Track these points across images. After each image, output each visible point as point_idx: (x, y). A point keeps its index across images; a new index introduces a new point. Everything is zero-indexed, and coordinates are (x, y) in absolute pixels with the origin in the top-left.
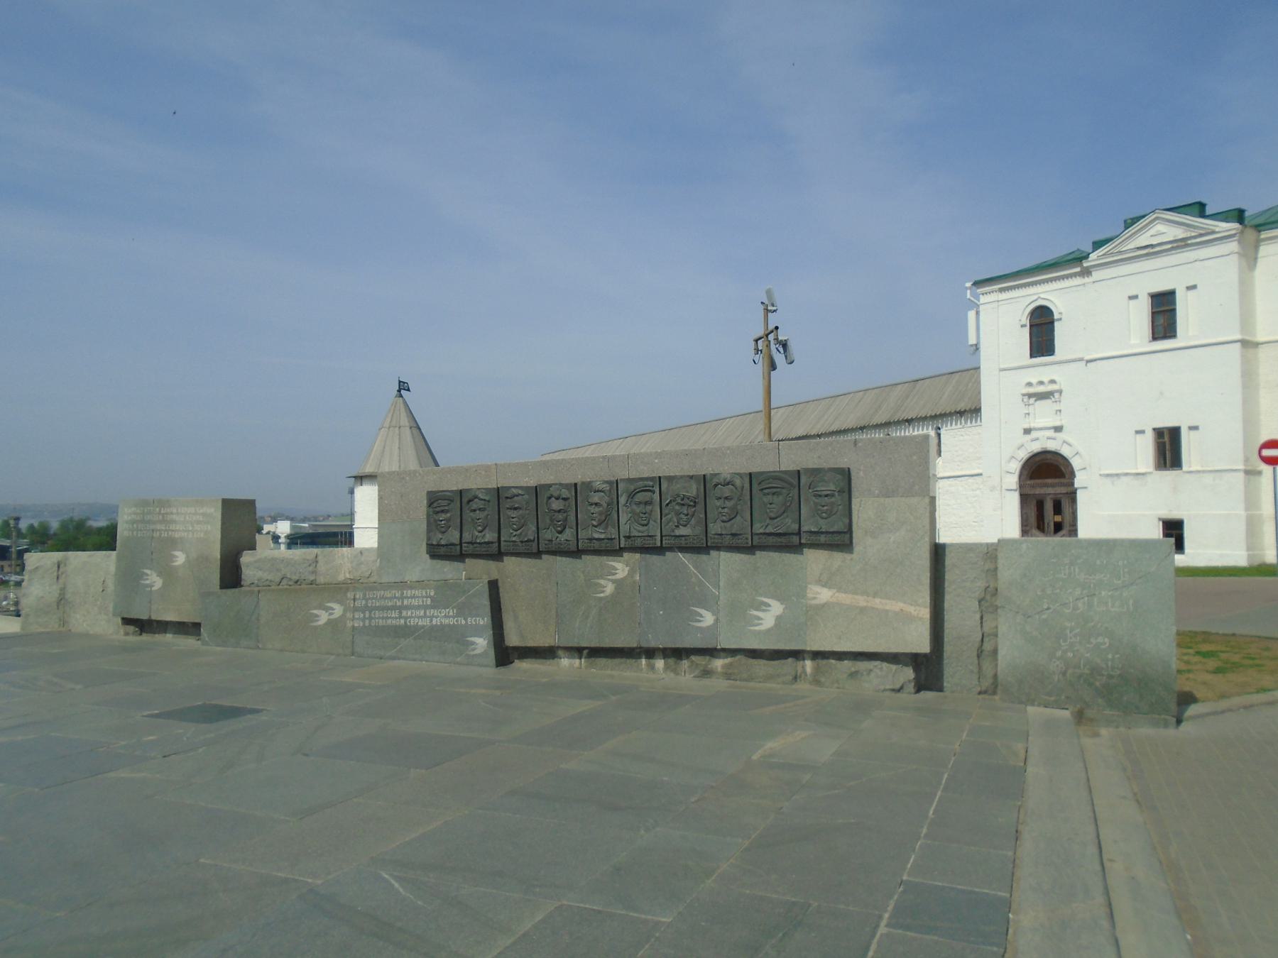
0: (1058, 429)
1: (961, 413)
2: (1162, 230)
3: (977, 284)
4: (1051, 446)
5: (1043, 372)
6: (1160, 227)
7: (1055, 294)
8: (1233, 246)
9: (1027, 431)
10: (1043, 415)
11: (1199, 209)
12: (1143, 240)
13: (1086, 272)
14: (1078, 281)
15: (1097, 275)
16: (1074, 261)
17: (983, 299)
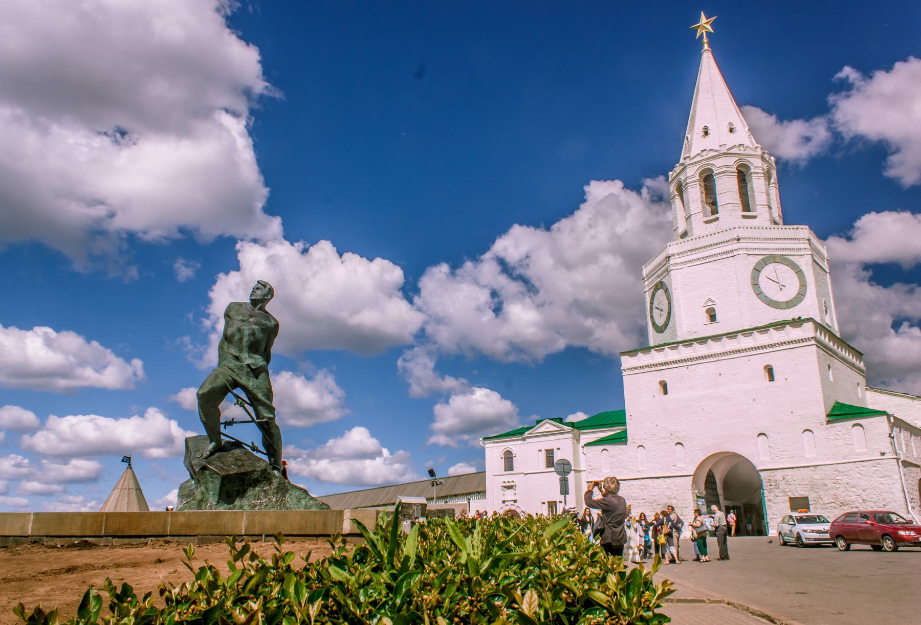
0: (515, 501)
1: (479, 493)
2: (548, 427)
3: (484, 439)
4: (513, 508)
5: (508, 478)
6: (548, 425)
7: (514, 446)
8: (570, 435)
9: (504, 502)
10: (509, 495)
11: (561, 420)
12: (543, 429)
13: (524, 439)
14: (521, 442)
15: (528, 440)
16: (518, 433)
17: (487, 445)
